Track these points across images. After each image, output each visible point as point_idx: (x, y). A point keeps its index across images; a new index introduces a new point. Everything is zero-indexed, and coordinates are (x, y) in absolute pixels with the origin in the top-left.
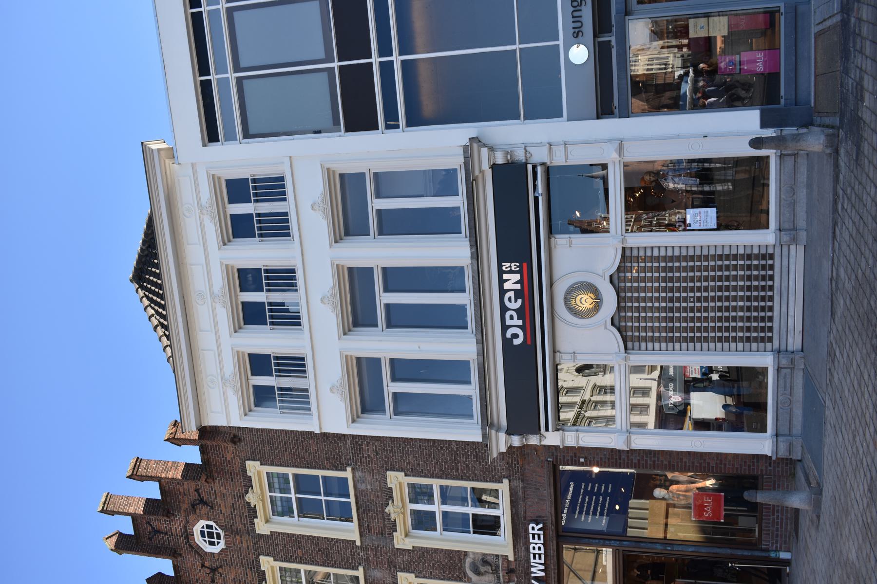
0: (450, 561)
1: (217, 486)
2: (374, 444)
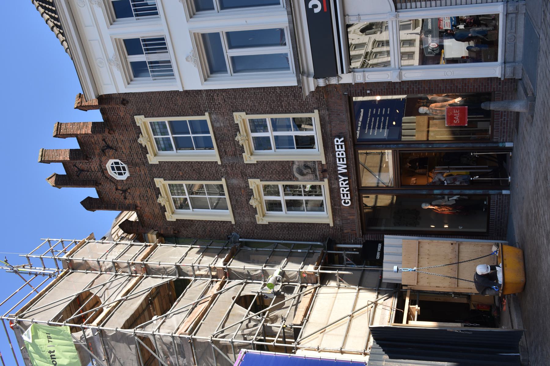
0: (282, 168)
1: (116, 135)
2: (222, 95)
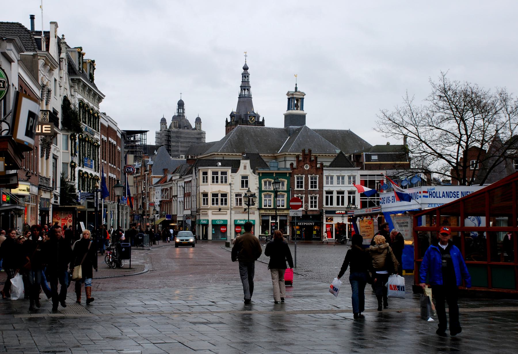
1: (314, 169)
